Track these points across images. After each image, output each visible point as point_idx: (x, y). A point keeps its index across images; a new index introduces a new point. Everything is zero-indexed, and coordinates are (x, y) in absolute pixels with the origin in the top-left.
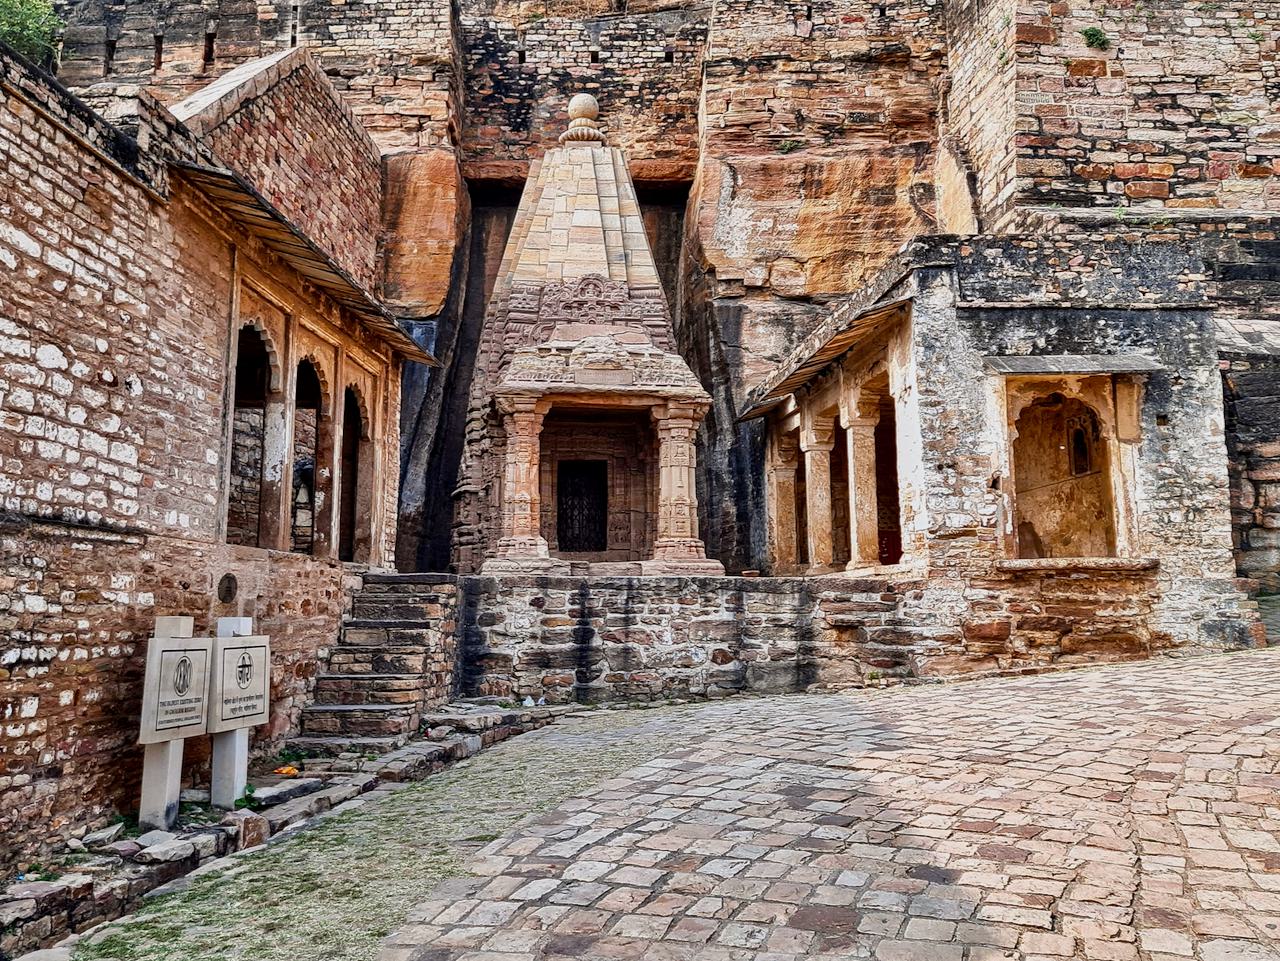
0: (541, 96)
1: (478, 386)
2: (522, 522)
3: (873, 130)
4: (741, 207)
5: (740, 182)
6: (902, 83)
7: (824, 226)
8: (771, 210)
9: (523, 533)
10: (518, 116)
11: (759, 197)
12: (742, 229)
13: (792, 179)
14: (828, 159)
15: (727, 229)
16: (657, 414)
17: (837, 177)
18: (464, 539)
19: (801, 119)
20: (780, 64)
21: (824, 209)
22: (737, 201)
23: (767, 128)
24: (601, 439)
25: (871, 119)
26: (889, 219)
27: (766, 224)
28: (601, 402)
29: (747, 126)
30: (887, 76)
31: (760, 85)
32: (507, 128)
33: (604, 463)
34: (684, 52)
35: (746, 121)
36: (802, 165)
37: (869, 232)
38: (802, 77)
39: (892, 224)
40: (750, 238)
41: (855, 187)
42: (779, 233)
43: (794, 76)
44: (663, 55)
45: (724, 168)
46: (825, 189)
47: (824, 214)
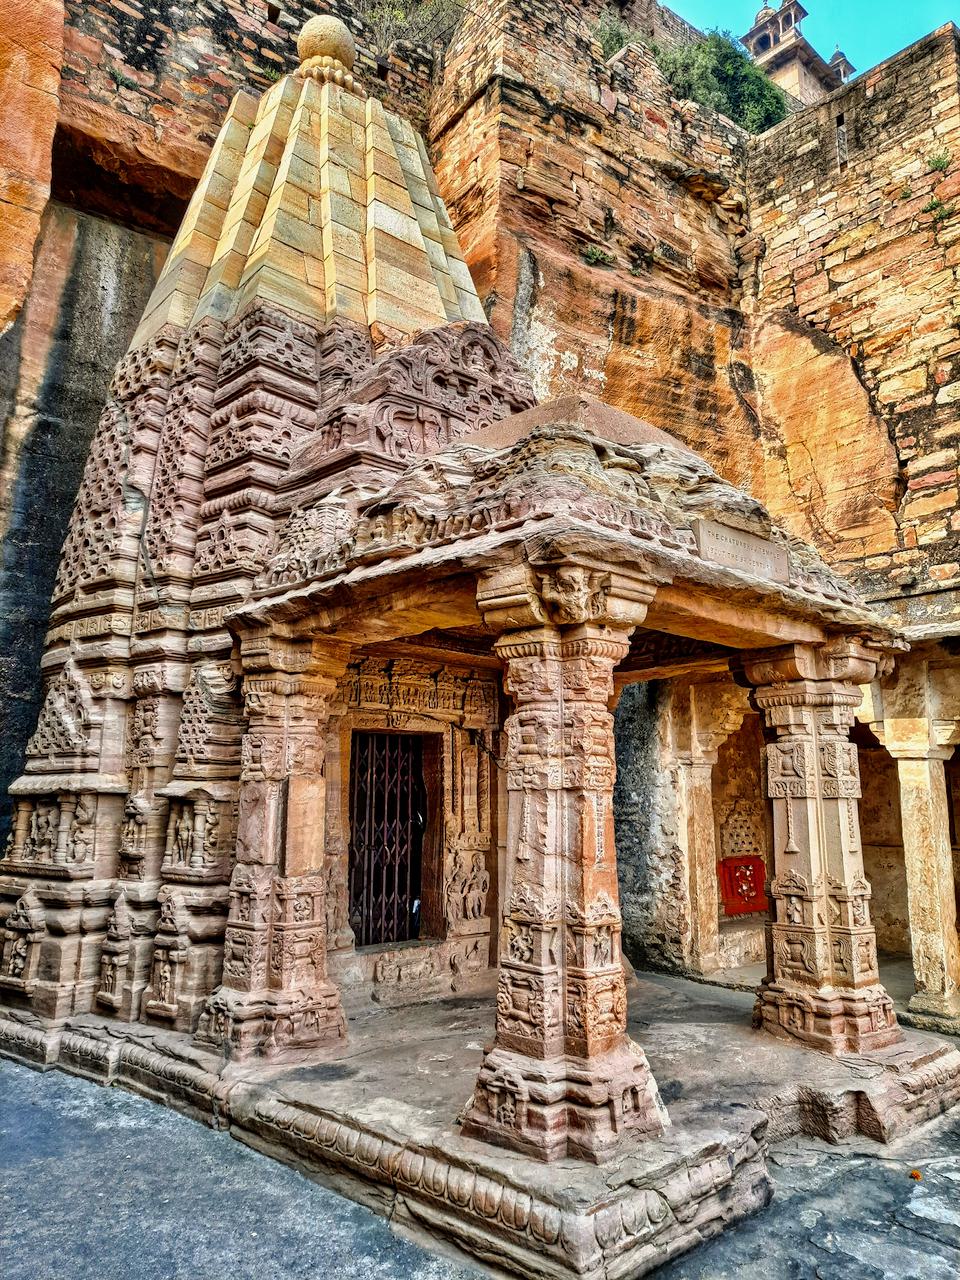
0: (184, 29)
1: (129, 529)
2: (606, 1000)
3: (680, 276)
4: (542, 321)
5: (542, 284)
6: (706, 228)
7: (639, 387)
8: (576, 341)
9: (610, 1044)
10: (141, 41)
11: (562, 316)
12: (545, 357)
13: (597, 304)
14: (640, 294)
15: (524, 350)
16: (804, 663)
17: (653, 321)
18: (68, 919)
19: (611, 224)
20: (591, 131)
21: (638, 362)
22: (537, 312)
23: (572, 215)
24: (446, 687)
25: (678, 259)
26: (711, 401)
27: (570, 360)
28: (729, 617)
29: (551, 201)
30: (692, 211)
31: (567, 150)
32: (116, 53)
33: (436, 739)
34: (404, 78)
35: (551, 194)
36: (612, 292)
37: (691, 411)
38: (613, 163)
39: (714, 408)
40: (553, 374)
41: (675, 342)
42: (585, 379)
43: (605, 158)
44: (374, 65)
45: (522, 252)
46: (639, 333)
47: (639, 369)
